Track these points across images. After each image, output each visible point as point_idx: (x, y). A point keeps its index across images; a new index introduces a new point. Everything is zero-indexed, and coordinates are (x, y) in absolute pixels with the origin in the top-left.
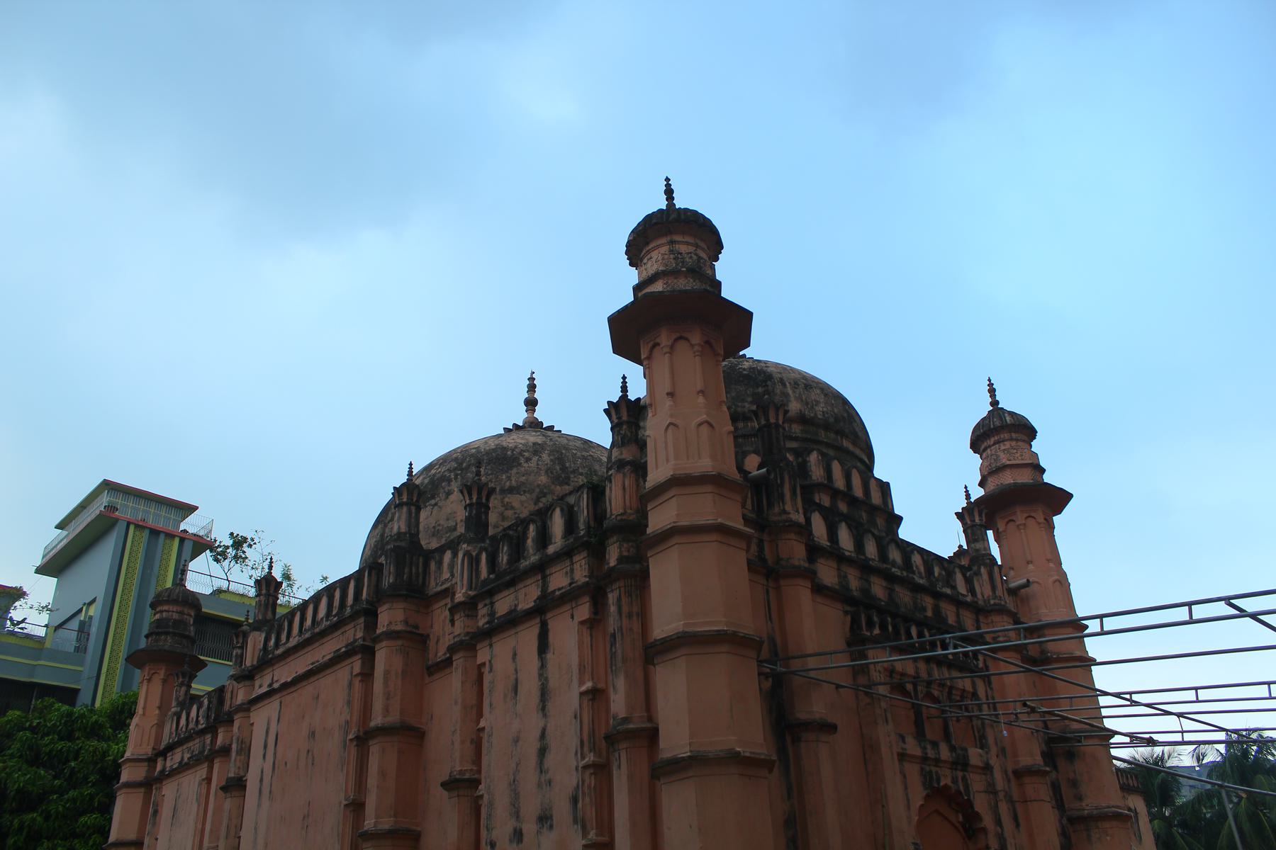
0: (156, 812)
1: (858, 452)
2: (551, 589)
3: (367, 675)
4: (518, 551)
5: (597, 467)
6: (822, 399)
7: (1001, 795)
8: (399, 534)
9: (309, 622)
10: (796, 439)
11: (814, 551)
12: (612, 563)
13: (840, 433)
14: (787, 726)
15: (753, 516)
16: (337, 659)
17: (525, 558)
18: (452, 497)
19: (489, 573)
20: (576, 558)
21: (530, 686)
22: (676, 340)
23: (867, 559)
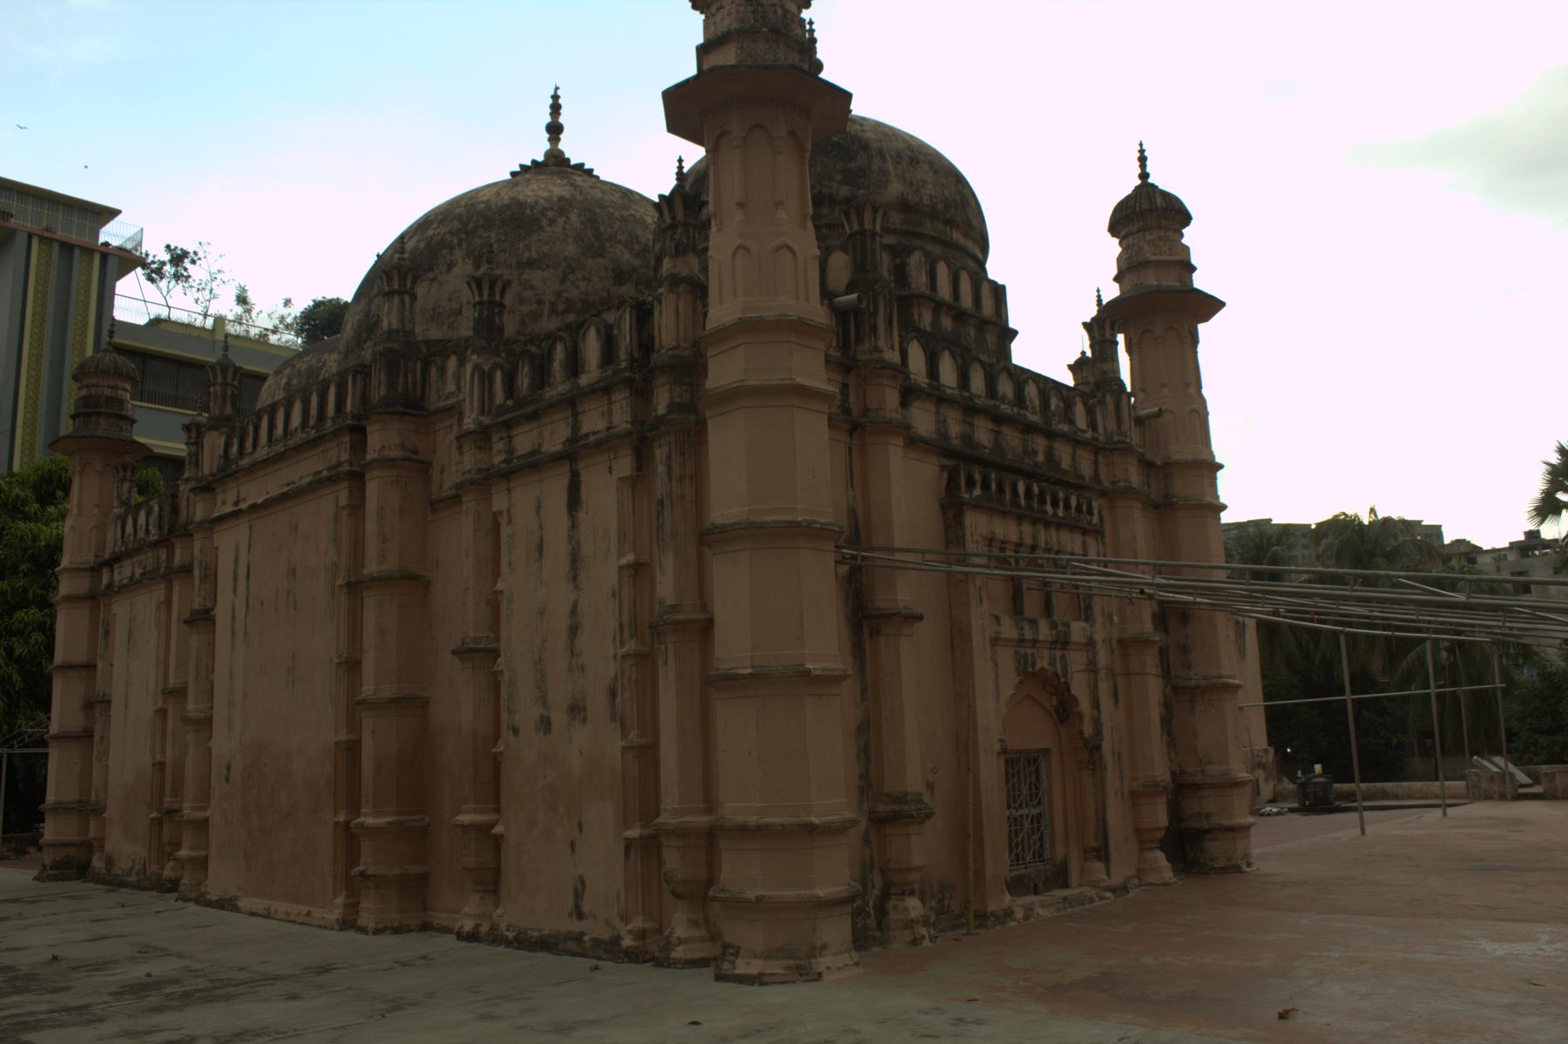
0: (107, 632)
2: (584, 429)
3: (357, 507)
4: (542, 376)
5: (639, 232)
7: (1102, 673)
8: (390, 332)
9: (279, 430)
10: (894, 232)
11: (909, 394)
12: (661, 410)
14: (866, 619)
16: (318, 484)
18: (456, 271)
20: (616, 397)
21: (557, 548)
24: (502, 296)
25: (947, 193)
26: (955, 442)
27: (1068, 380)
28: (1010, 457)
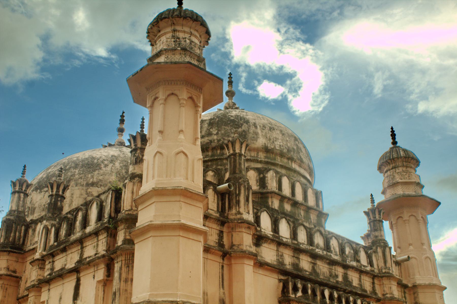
1: (302, 171)
2: (85, 256)
4: (70, 231)
6: (280, 136)
10: (261, 162)
11: (259, 239)
12: (120, 243)
13: (291, 159)
17: (73, 234)
19: (55, 242)
20: (101, 237)
22: (169, 95)
23: (299, 244)
24: (63, 193)
25: (289, 145)
26: (288, 267)
27: (362, 243)
28: (321, 277)
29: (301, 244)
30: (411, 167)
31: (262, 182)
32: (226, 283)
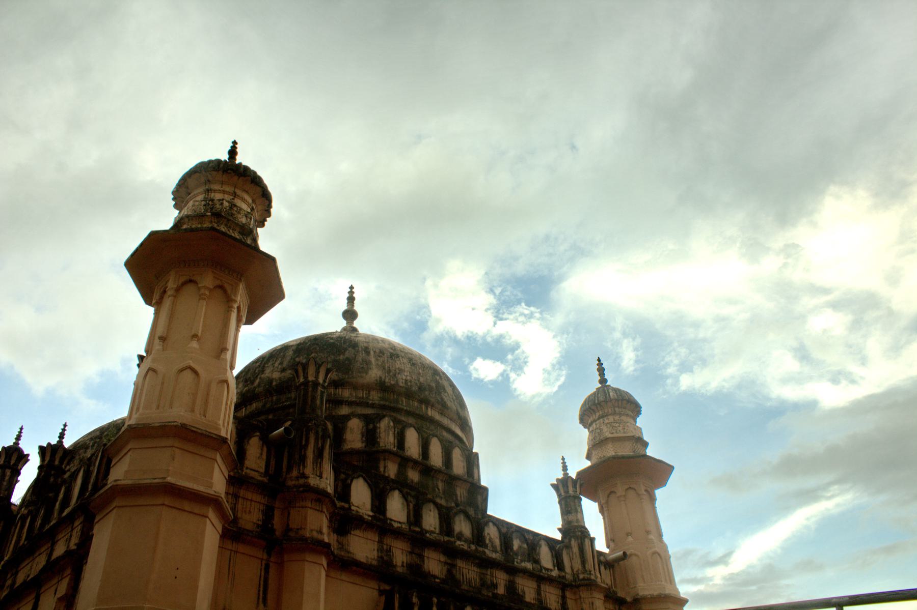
1: (446, 421)
6: (408, 367)
10: (372, 406)
11: (344, 522)
13: (426, 402)
15: (265, 480)
23: (423, 532)
25: (422, 380)
26: (400, 570)
29: (427, 532)
30: (627, 415)
31: (371, 436)
32: (271, 596)
